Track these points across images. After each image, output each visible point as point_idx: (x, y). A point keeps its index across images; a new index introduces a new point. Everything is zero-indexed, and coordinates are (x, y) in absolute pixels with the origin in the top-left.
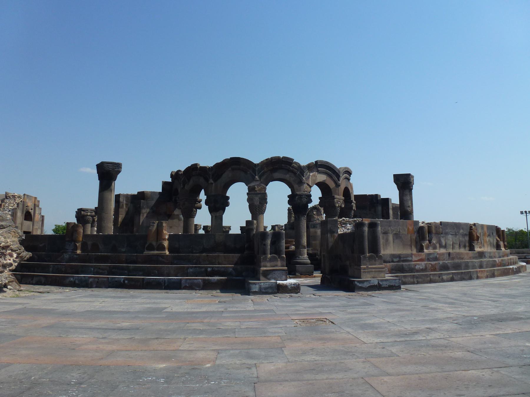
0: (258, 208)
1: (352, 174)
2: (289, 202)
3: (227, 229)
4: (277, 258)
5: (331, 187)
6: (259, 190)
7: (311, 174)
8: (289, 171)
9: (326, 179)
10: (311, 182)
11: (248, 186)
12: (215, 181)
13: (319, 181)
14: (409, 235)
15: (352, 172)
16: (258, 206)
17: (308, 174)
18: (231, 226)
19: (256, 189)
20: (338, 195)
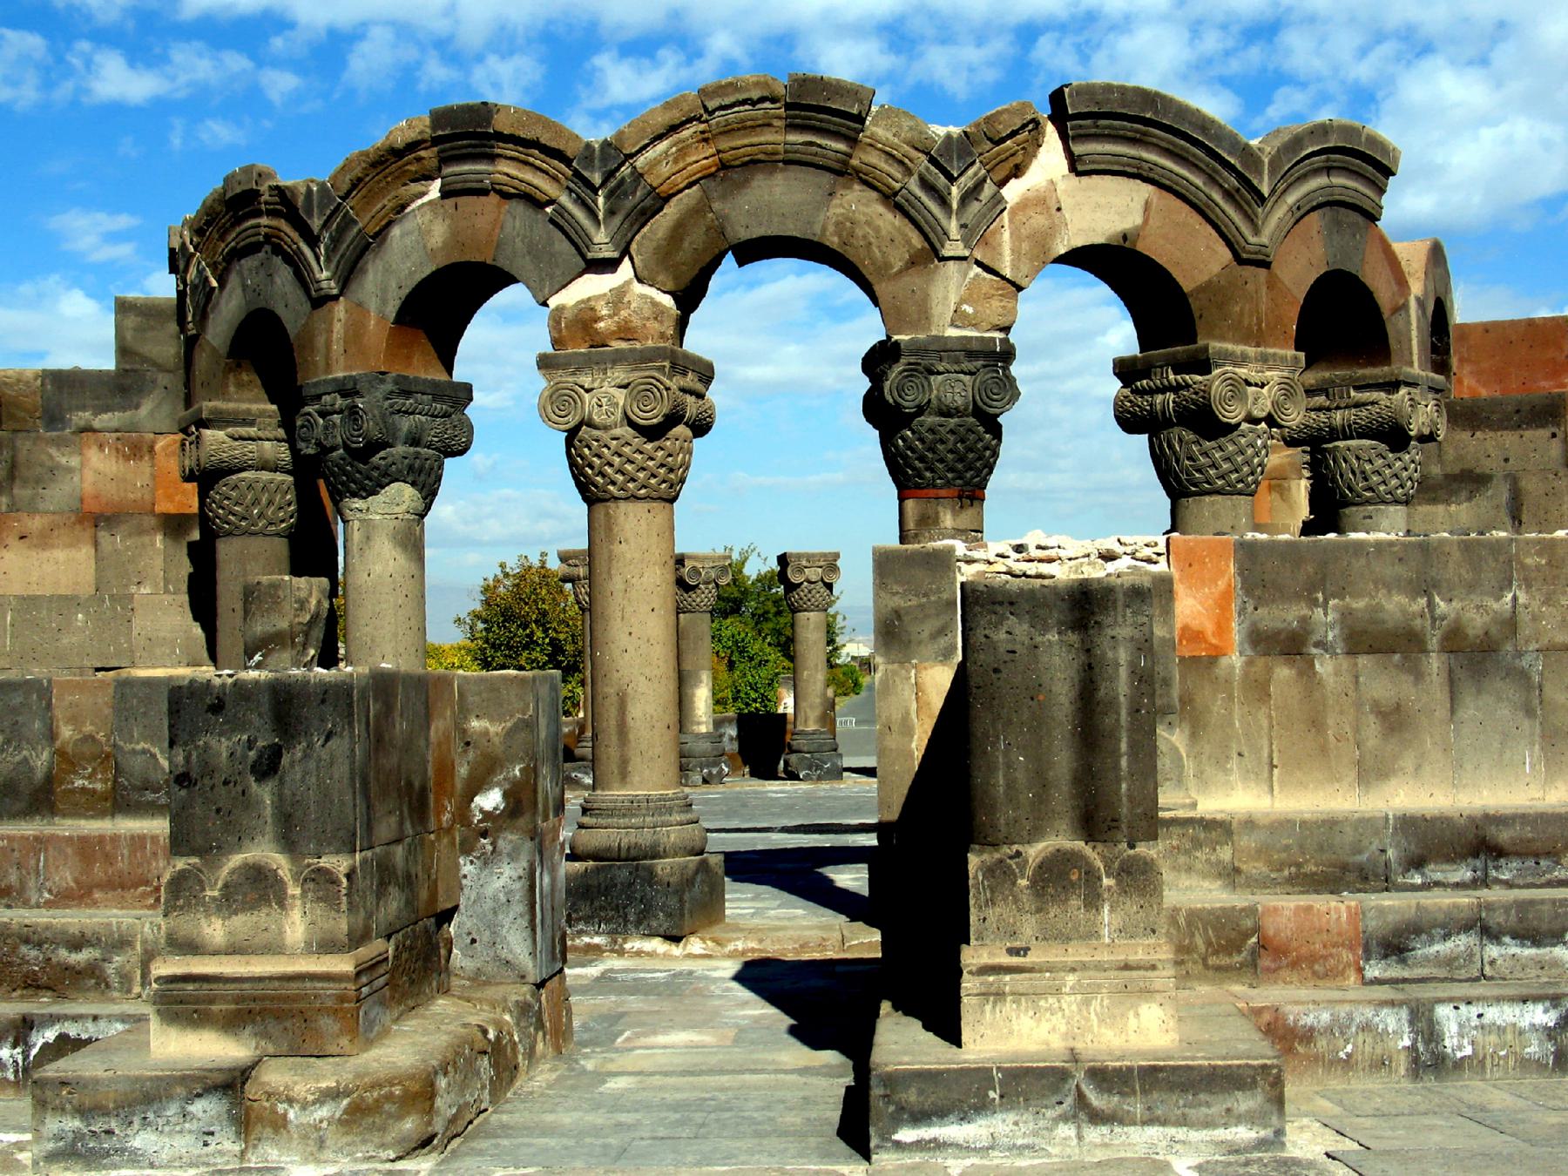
0: (617, 460)
1: (1401, 169)
2: (876, 409)
3: (814, 574)
4: (279, 884)
5: (1187, 285)
7: (1013, 191)
9: (1138, 220)
10: (1013, 251)
11: (553, 302)
12: (348, 275)
13: (1079, 242)
15: (1393, 154)
17: (988, 189)
18: (837, 556)
19: (602, 325)
20: (1246, 338)
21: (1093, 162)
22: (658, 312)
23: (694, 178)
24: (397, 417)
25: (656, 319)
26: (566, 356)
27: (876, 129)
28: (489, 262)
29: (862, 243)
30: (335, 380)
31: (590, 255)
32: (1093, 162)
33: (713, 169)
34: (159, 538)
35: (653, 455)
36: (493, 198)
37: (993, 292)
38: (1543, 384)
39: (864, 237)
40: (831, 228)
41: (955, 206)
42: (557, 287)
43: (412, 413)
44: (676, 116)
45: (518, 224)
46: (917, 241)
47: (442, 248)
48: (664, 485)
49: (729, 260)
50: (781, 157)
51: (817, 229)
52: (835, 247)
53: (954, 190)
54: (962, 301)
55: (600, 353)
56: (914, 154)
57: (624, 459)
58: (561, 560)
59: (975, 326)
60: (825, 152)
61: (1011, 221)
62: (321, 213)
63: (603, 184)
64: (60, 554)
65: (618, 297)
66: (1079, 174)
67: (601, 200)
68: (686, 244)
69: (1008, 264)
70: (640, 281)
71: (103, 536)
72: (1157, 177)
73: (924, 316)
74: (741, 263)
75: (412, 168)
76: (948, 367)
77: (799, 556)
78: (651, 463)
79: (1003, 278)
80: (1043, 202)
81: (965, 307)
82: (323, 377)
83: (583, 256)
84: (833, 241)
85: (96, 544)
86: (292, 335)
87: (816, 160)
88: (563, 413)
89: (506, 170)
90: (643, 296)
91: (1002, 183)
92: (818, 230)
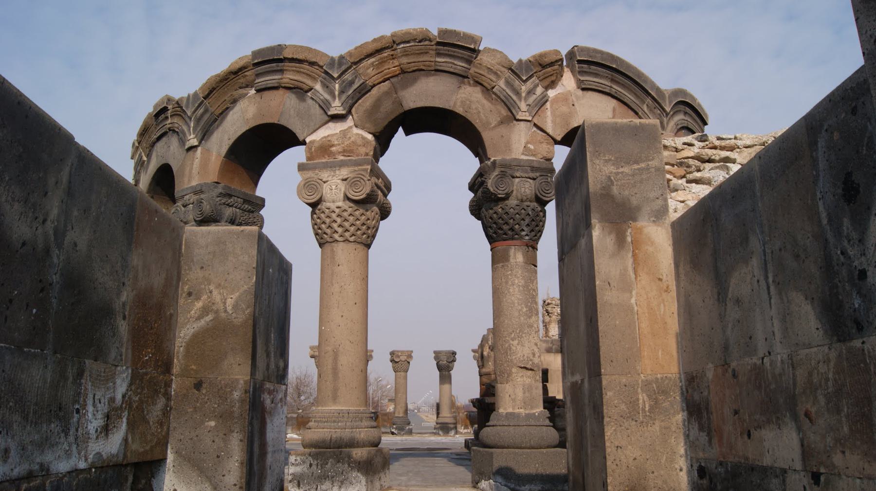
0: (339, 220)
3: (403, 358)
6: (344, 152)
7: (551, 93)
8: (462, 77)
10: (552, 121)
12: (205, 135)
16: (337, 211)
17: (539, 90)
18: (412, 352)
19: (334, 149)
21: (589, 85)
22: (366, 142)
23: (387, 76)
24: (223, 206)
25: (364, 146)
26: (313, 164)
27: (483, 59)
28: (276, 122)
29: (475, 111)
30: (192, 187)
31: (330, 113)
32: (589, 85)
33: (398, 72)
35: (360, 218)
36: (281, 92)
37: (542, 140)
39: (476, 109)
40: (459, 104)
41: (524, 95)
42: (310, 133)
43: (232, 206)
44: (378, 45)
45: (292, 102)
46: (504, 112)
47: (253, 118)
48: (365, 236)
49: (401, 129)
50: (433, 68)
51: (452, 104)
52: (461, 113)
53: (523, 88)
54: (527, 143)
55: (333, 162)
56: (503, 69)
57: (343, 219)
58: (310, 348)
59: (534, 155)
60: (456, 66)
61: (551, 107)
62: (193, 105)
63: (339, 77)
65: (344, 133)
66: (583, 89)
67: (337, 86)
68: (381, 110)
69: (550, 127)
70: (356, 127)
72: (619, 97)
74: (407, 133)
75: (242, 80)
76: (522, 174)
77: (398, 351)
78: (358, 222)
79: (548, 134)
80: (564, 98)
81: (529, 145)
83: (326, 113)
84: (460, 110)
86: (174, 173)
87: (452, 70)
88: (311, 194)
89: (290, 77)
90: (357, 134)
91: (547, 88)
92: (452, 104)
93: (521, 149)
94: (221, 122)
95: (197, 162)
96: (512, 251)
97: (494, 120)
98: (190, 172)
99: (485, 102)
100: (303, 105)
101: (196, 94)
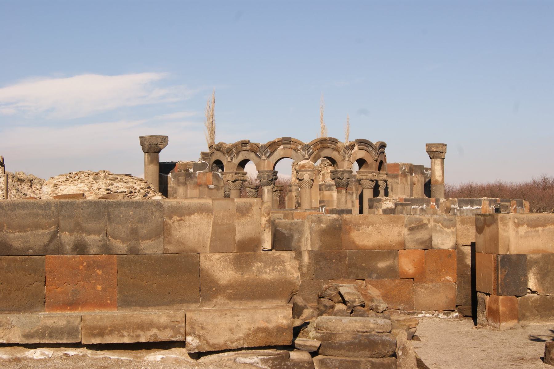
8: (334, 149)
10: (353, 159)
13: (358, 158)
14: (432, 210)
15: (386, 145)
17: (350, 152)
19: (306, 167)
34: (207, 188)
36: (290, 149)
38: (396, 172)
64: (195, 191)
71: (200, 188)
73: (343, 167)
82: (263, 170)
84: (333, 158)
85: (199, 189)
89: (292, 146)
91: (351, 151)
93: (346, 167)
94: (273, 154)
95: (266, 164)
96: (343, 190)
97: (340, 160)
98: (264, 166)
99: (338, 155)
100: (297, 154)
101: (264, 146)
